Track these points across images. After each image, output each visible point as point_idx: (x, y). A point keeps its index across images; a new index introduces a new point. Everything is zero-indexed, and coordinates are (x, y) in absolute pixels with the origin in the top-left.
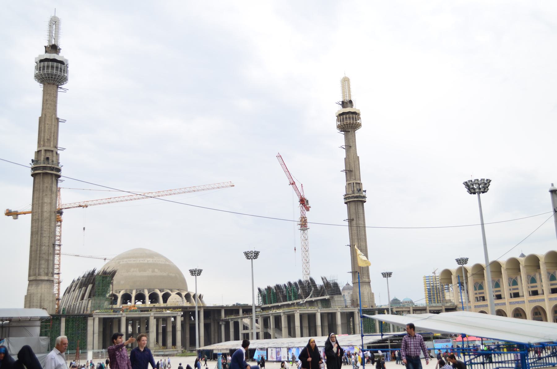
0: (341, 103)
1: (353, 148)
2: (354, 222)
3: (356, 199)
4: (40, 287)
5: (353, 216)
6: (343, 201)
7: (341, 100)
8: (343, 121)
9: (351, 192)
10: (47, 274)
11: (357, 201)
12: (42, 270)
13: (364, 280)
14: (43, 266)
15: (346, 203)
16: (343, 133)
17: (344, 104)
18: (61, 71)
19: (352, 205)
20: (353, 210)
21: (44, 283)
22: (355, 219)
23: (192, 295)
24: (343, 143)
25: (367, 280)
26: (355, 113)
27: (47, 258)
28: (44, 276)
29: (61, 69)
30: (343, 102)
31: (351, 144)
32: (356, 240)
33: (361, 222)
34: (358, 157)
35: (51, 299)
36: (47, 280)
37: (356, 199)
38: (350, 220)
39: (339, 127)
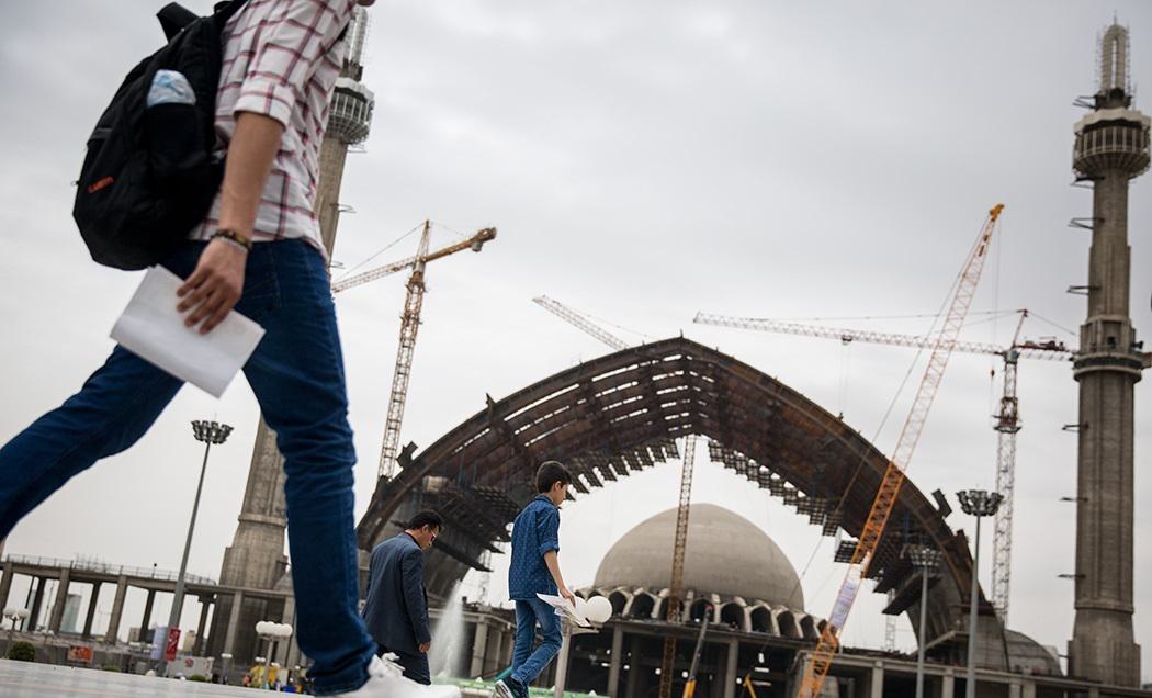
0: (1092, 102)
1: (1110, 224)
2: (1090, 434)
3: (1094, 368)
4: (245, 535)
5: (1089, 418)
6: (1072, 373)
7: (1092, 86)
8: (1082, 150)
9: (1088, 347)
10: (263, 511)
11: (1103, 372)
12: (255, 502)
13: (1102, 601)
14: (258, 494)
15: (1077, 378)
16: (1091, 184)
17: (1101, 102)
18: (356, 115)
19: (1090, 381)
20: (1089, 401)
21: (256, 527)
22: (1091, 425)
23: (816, 622)
24: (1086, 211)
25: (1112, 603)
26: (1121, 122)
27: (268, 478)
28: (258, 513)
29: (357, 109)
30: (1096, 97)
31: (1106, 213)
32: (1089, 486)
33: (1111, 433)
34: (1128, 249)
35: (265, 560)
36: (262, 523)
37: (1094, 368)
38: (1083, 427)
39: (1077, 165)
